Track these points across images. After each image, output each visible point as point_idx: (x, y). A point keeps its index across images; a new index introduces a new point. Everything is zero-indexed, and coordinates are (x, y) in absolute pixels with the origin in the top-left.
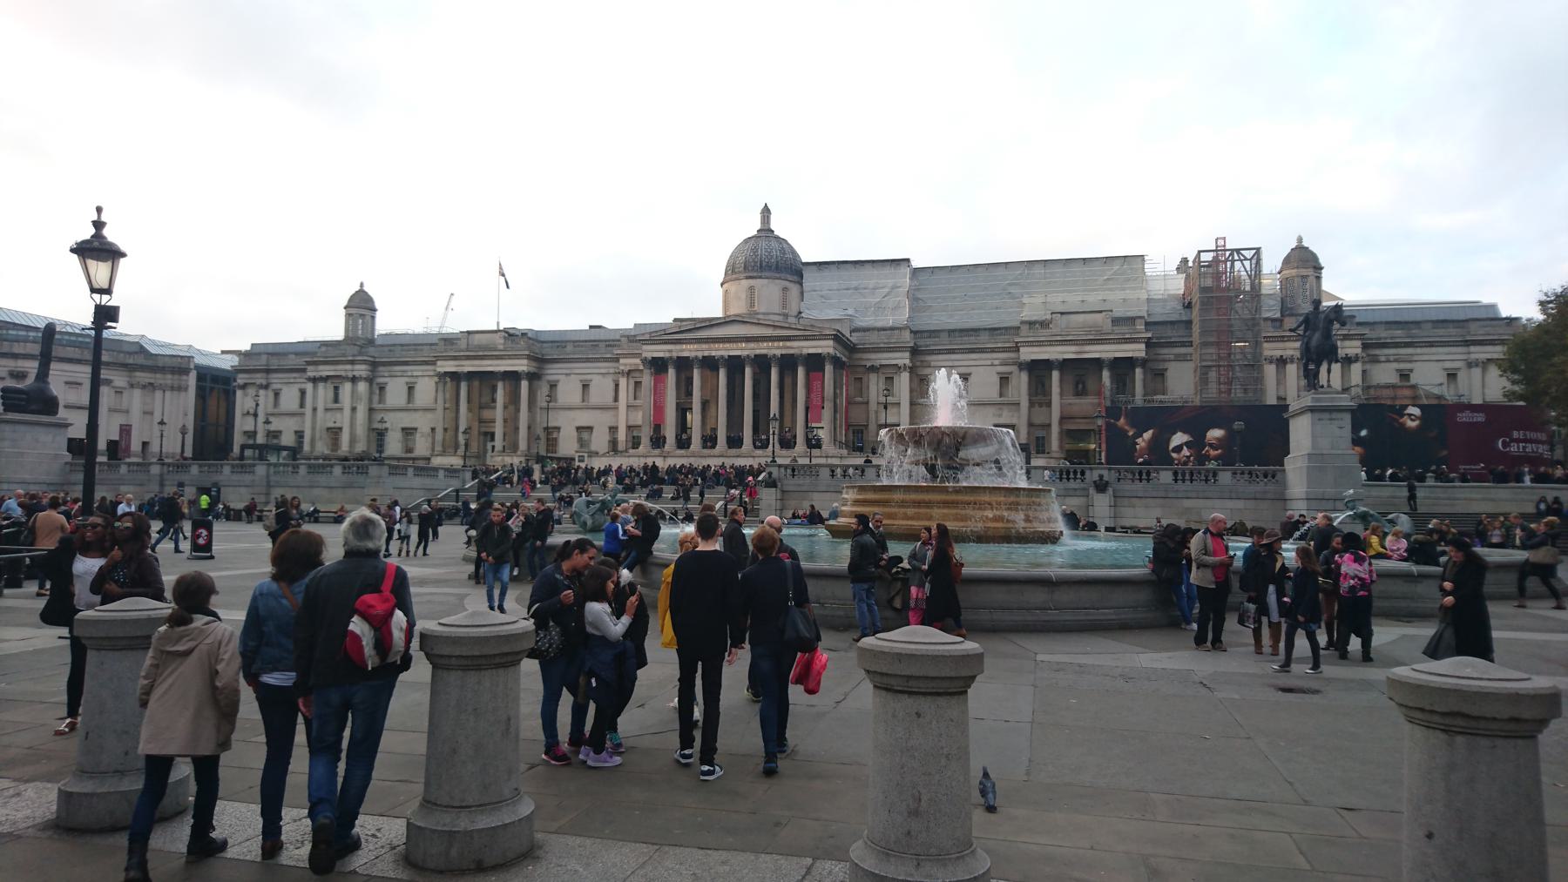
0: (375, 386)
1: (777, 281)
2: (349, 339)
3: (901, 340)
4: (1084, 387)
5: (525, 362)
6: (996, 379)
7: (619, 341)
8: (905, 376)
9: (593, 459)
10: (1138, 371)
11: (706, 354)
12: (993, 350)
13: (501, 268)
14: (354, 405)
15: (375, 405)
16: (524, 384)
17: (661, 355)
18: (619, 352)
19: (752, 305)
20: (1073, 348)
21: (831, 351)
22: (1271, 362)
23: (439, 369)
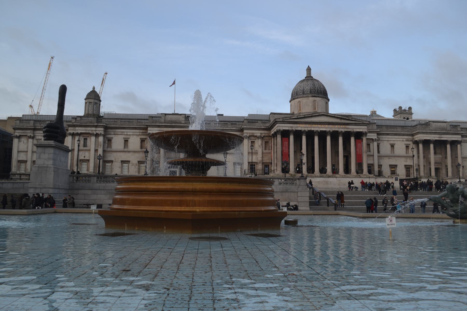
0: (105, 139)
1: (324, 99)
2: (87, 115)
3: (372, 128)
6: (404, 147)
7: (243, 122)
8: (375, 144)
10: (459, 146)
11: (309, 129)
12: (403, 135)
14: (97, 148)
15: (106, 149)
17: (287, 129)
18: (245, 127)
19: (315, 109)
23: (149, 132)
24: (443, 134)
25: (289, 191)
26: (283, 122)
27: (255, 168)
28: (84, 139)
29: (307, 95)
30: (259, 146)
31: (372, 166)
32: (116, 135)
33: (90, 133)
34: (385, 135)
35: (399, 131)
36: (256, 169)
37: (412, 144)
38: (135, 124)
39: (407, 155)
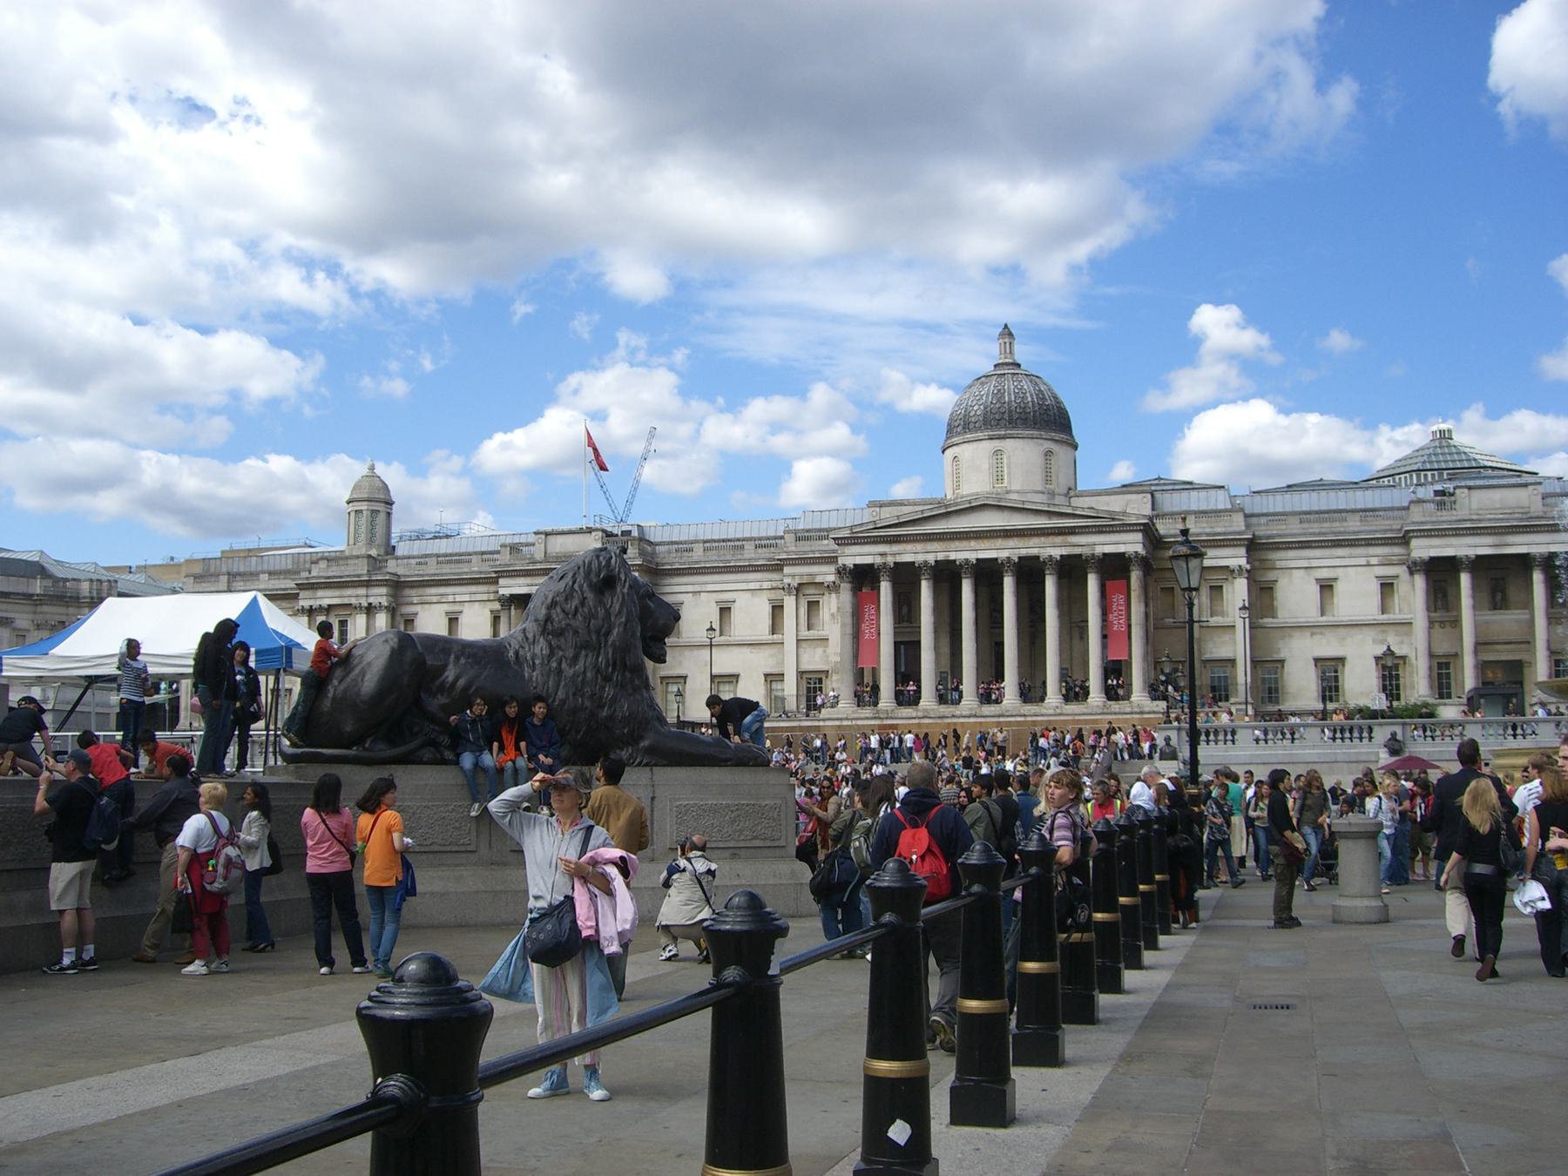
0: (398, 618)
3: (1230, 529)
4: (1504, 599)
6: (1375, 587)
7: (782, 538)
11: (941, 557)
12: (1369, 543)
17: (868, 560)
20: (1489, 540)
21: (1140, 549)
23: (502, 591)
24: (1509, 533)
26: (853, 540)
31: (1230, 665)
32: (427, 606)
34: (1296, 548)
35: (1352, 529)
38: (476, 569)
39: (1385, 616)
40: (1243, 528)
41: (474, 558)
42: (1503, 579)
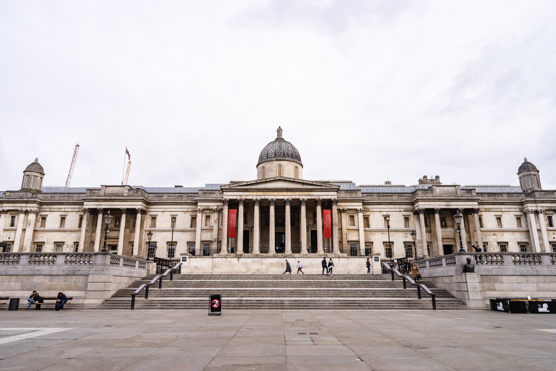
0: (39, 216)
2: (23, 190)
3: (356, 197)
5: (141, 203)
6: (402, 219)
7: (197, 193)
8: (361, 215)
9: (192, 259)
11: (263, 197)
12: (400, 204)
13: (127, 150)
14: (24, 228)
15: (37, 228)
16: (139, 216)
17: (235, 198)
22: (532, 213)
23: (85, 207)
25: (78, 273)
26: (230, 190)
27: (209, 247)
28: (12, 216)
29: (271, 159)
30: (215, 221)
31: (357, 243)
33: (18, 210)
34: (376, 205)
35: (394, 199)
36: (210, 248)
37: (413, 215)
38: (75, 199)
39: (407, 228)
40: (361, 196)
41: (75, 195)
42: (445, 218)
